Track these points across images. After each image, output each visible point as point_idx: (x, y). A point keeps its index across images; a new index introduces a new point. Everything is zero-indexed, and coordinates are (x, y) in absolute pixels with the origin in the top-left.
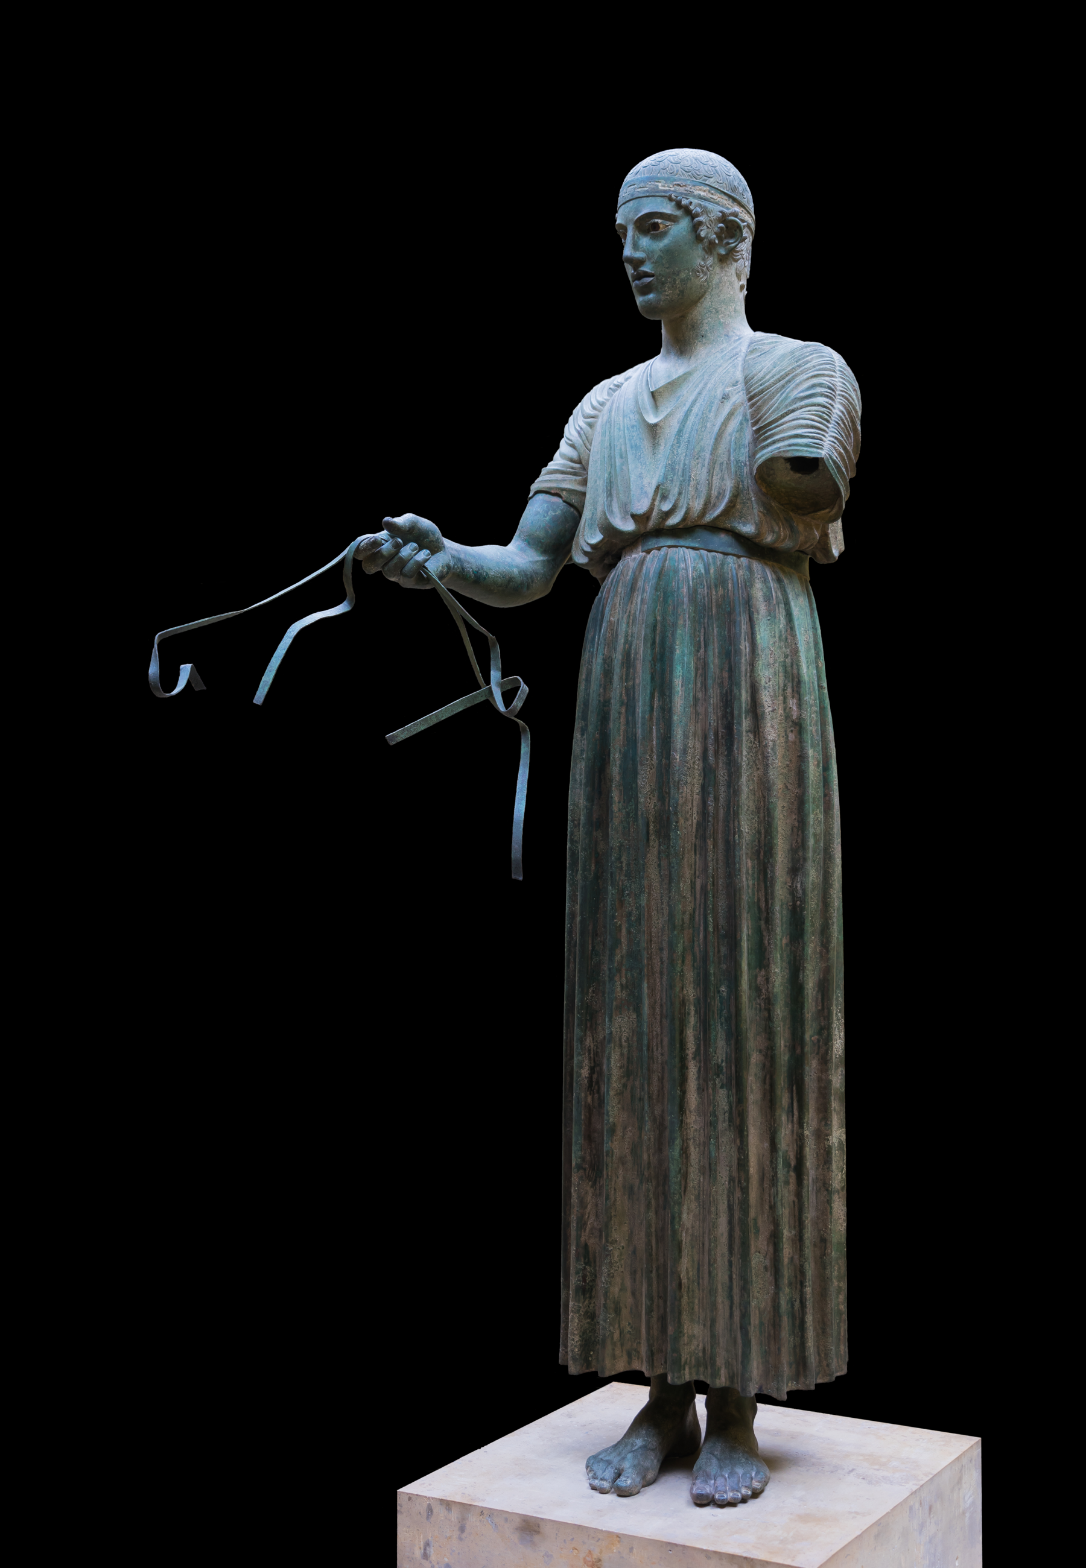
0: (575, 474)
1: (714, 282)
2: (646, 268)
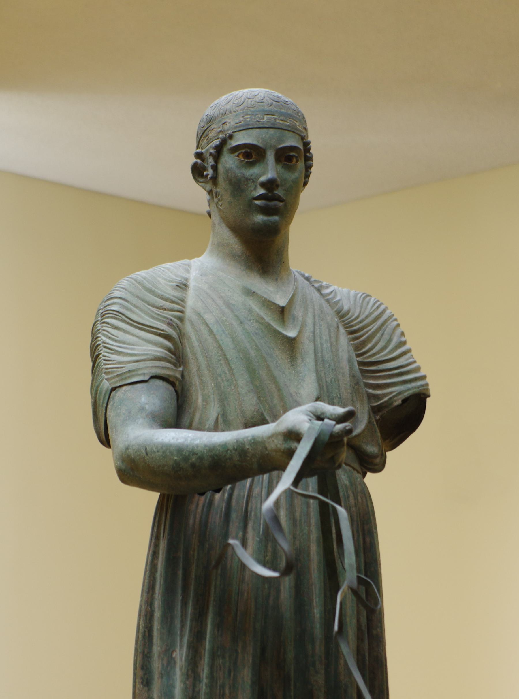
0: (175, 365)
2: (279, 192)
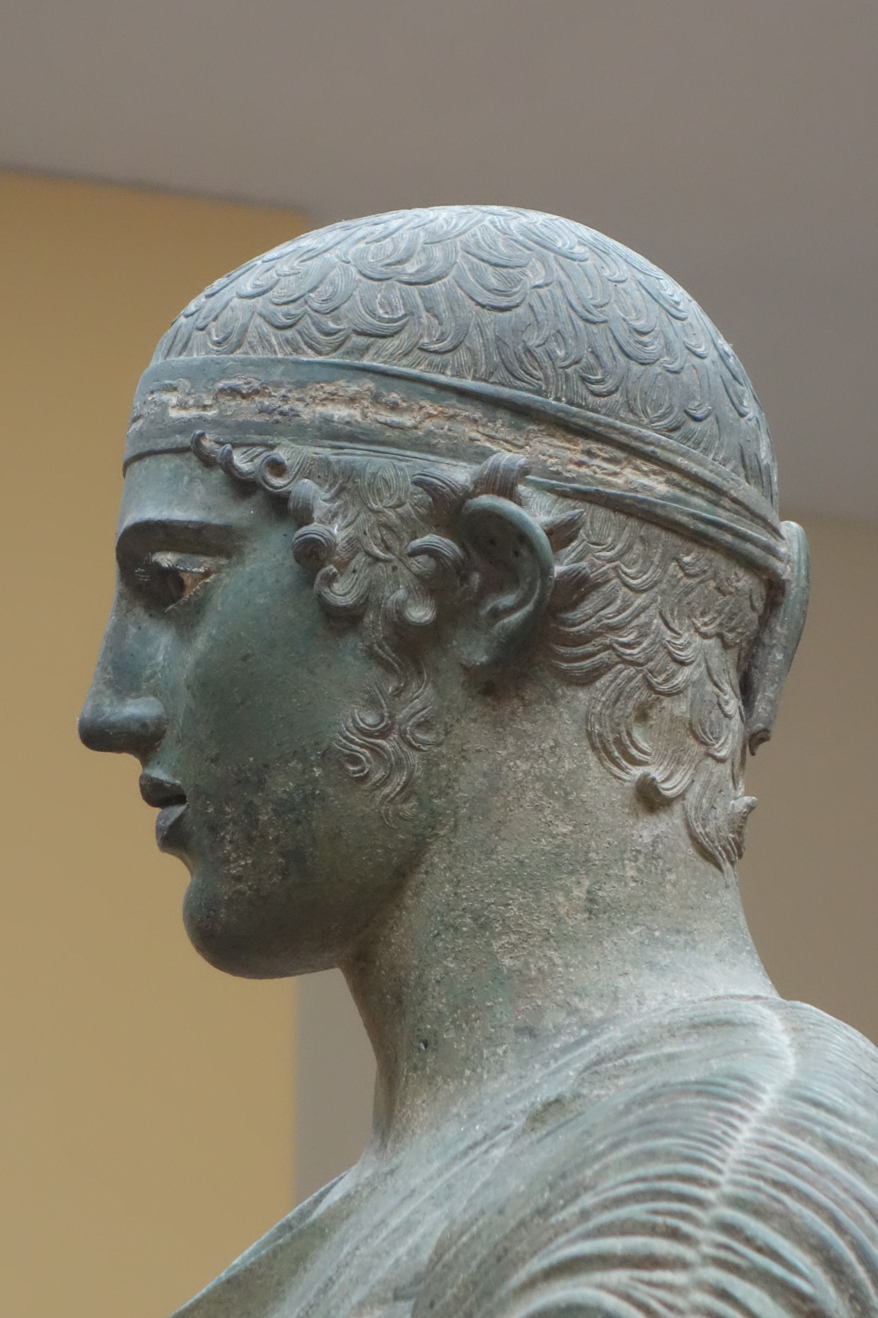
1: (463, 790)
